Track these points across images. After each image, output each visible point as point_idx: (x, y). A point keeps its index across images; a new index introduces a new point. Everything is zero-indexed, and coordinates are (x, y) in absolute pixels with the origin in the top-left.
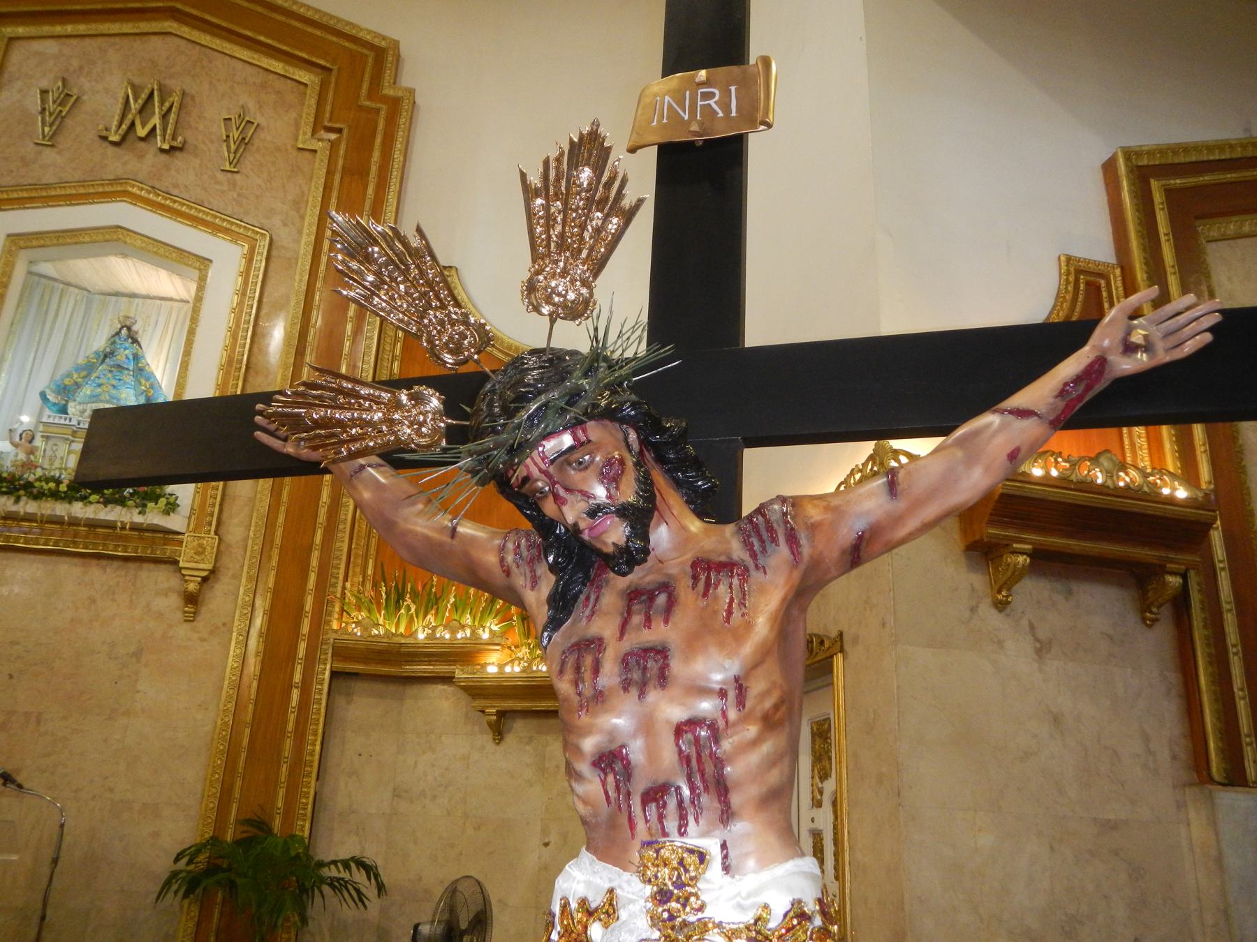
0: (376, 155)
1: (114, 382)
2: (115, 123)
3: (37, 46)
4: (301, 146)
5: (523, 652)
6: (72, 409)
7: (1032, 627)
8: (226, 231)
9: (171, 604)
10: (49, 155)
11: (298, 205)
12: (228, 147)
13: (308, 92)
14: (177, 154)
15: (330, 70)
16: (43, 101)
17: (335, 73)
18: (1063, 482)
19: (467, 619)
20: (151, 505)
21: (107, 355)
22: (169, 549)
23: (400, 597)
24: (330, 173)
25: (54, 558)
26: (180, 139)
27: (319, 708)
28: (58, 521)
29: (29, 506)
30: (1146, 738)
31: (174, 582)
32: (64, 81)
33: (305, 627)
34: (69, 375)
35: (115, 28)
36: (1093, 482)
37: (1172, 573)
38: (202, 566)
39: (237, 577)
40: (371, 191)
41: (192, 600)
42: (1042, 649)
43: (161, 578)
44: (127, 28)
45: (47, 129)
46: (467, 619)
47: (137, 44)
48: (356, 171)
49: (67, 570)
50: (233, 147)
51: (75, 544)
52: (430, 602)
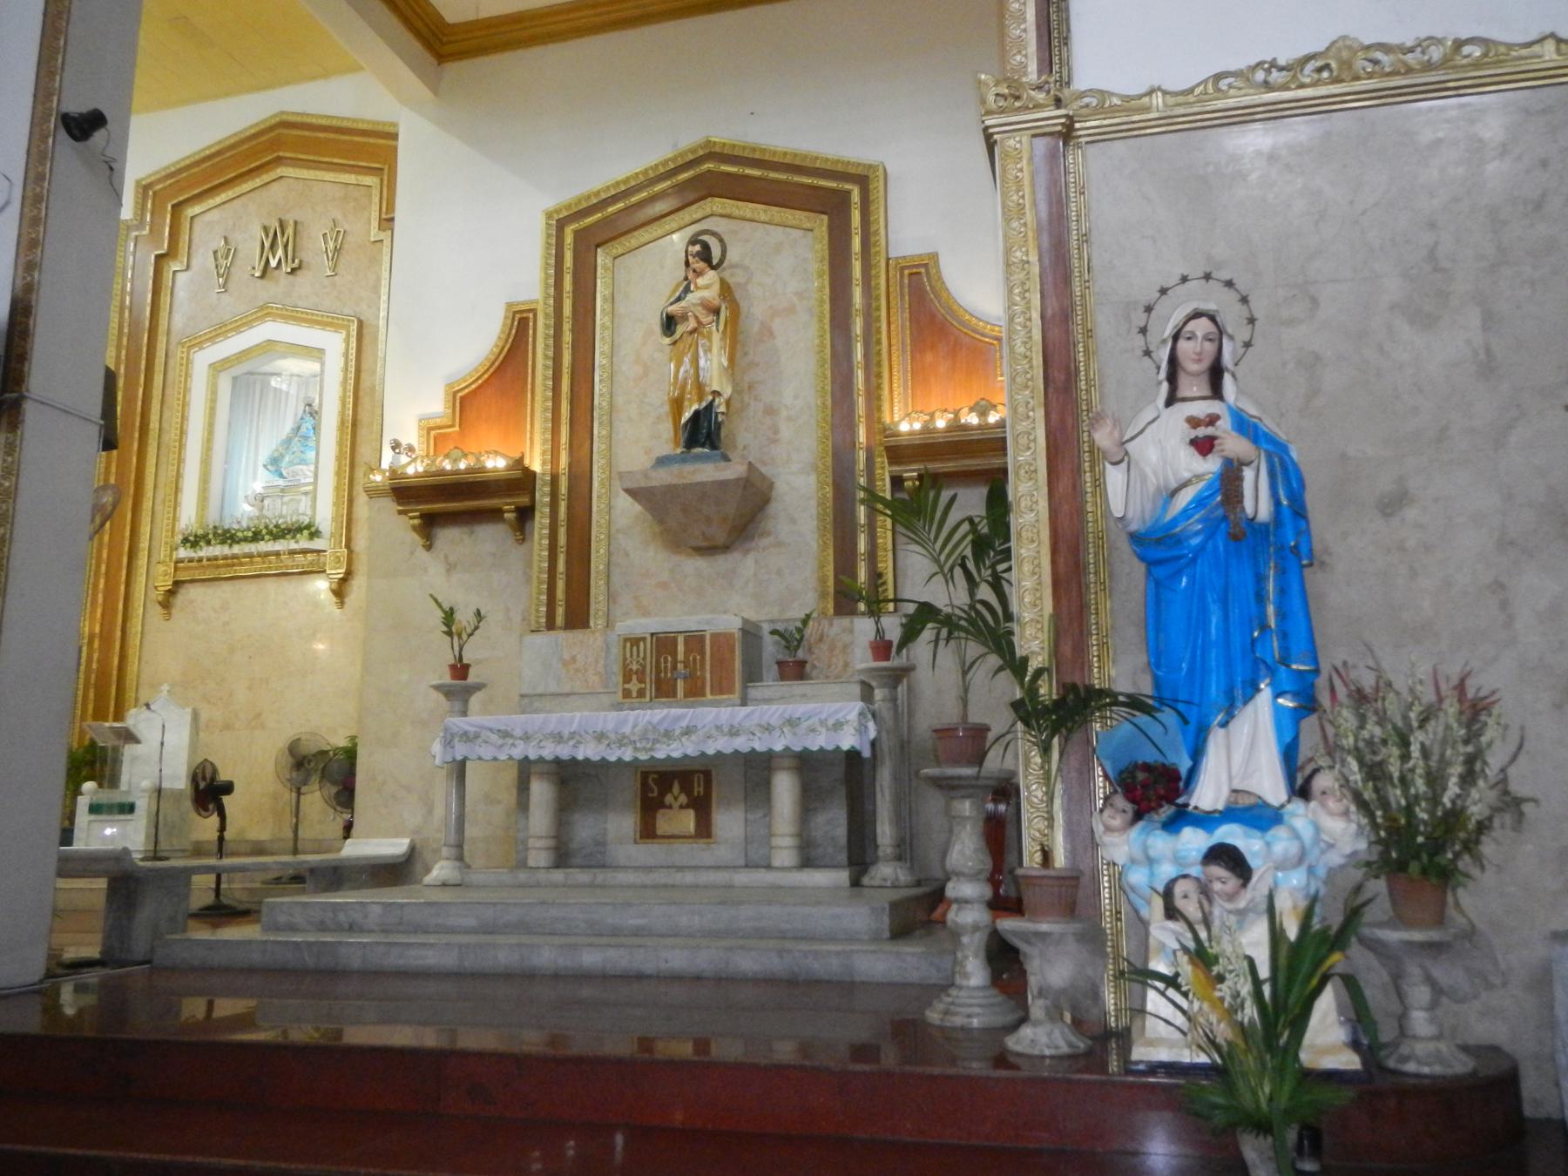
1: (303, 449)
2: (257, 263)
4: (372, 240)
7: (446, 557)
8: (330, 324)
10: (226, 298)
12: (328, 256)
13: (374, 192)
14: (299, 272)
15: (381, 169)
16: (216, 259)
17: (386, 171)
18: (427, 474)
20: (298, 536)
25: (257, 580)
26: (297, 261)
30: (508, 610)
32: (226, 239)
34: (277, 450)
35: (246, 187)
36: (443, 469)
37: (508, 511)
38: (339, 571)
42: (450, 568)
44: (258, 182)
45: (221, 280)
47: (264, 193)
50: (330, 255)
51: (270, 568)
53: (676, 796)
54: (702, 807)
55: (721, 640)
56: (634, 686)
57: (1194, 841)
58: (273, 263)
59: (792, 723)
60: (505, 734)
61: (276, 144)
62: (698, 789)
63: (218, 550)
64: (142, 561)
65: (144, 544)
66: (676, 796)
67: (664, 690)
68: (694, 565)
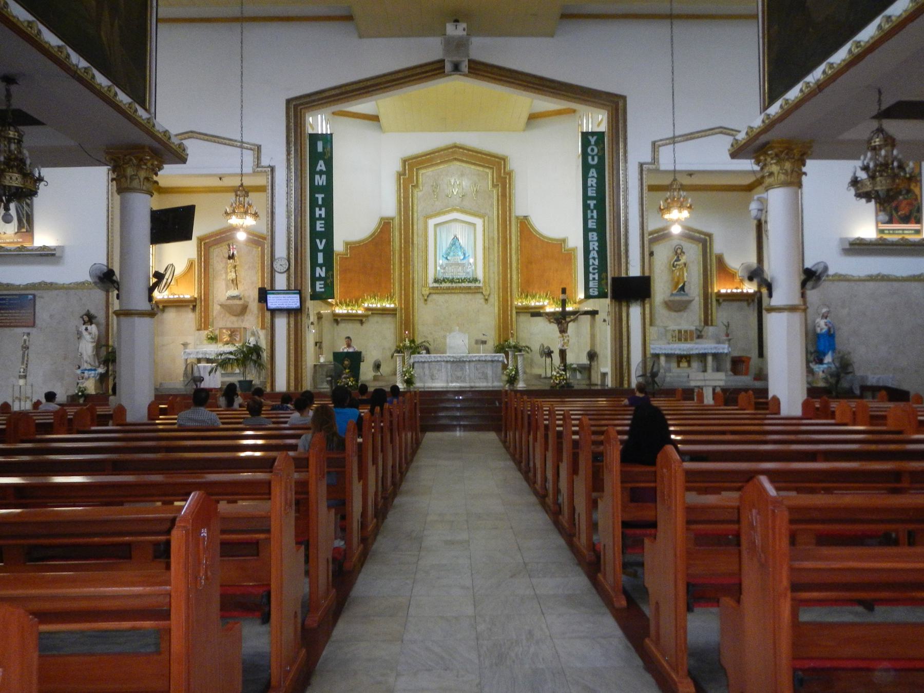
0: (508, 190)
3: (427, 174)
5: (554, 306)
6: (448, 258)
9: (482, 301)
10: (437, 203)
11: (492, 205)
19: (542, 300)
21: (453, 244)
22: (481, 291)
23: (527, 296)
24: (498, 196)
27: (514, 319)
28: (460, 287)
29: (454, 285)
31: (482, 296)
33: (509, 303)
39: (494, 294)
40: (508, 200)
41: (486, 300)
43: (480, 296)
46: (542, 300)
48: (504, 195)
49: (462, 296)
52: (533, 297)
53: (684, 360)
54: (689, 362)
55: (691, 332)
56: (674, 339)
57: (825, 366)
58: (455, 193)
59: (716, 348)
60: (661, 348)
61: (453, 153)
62: (688, 359)
63: (448, 285)
64: (416, 286)
65: (416, 280)
66: (684, 360)
67: (680, 340)
68: (673, 314)
